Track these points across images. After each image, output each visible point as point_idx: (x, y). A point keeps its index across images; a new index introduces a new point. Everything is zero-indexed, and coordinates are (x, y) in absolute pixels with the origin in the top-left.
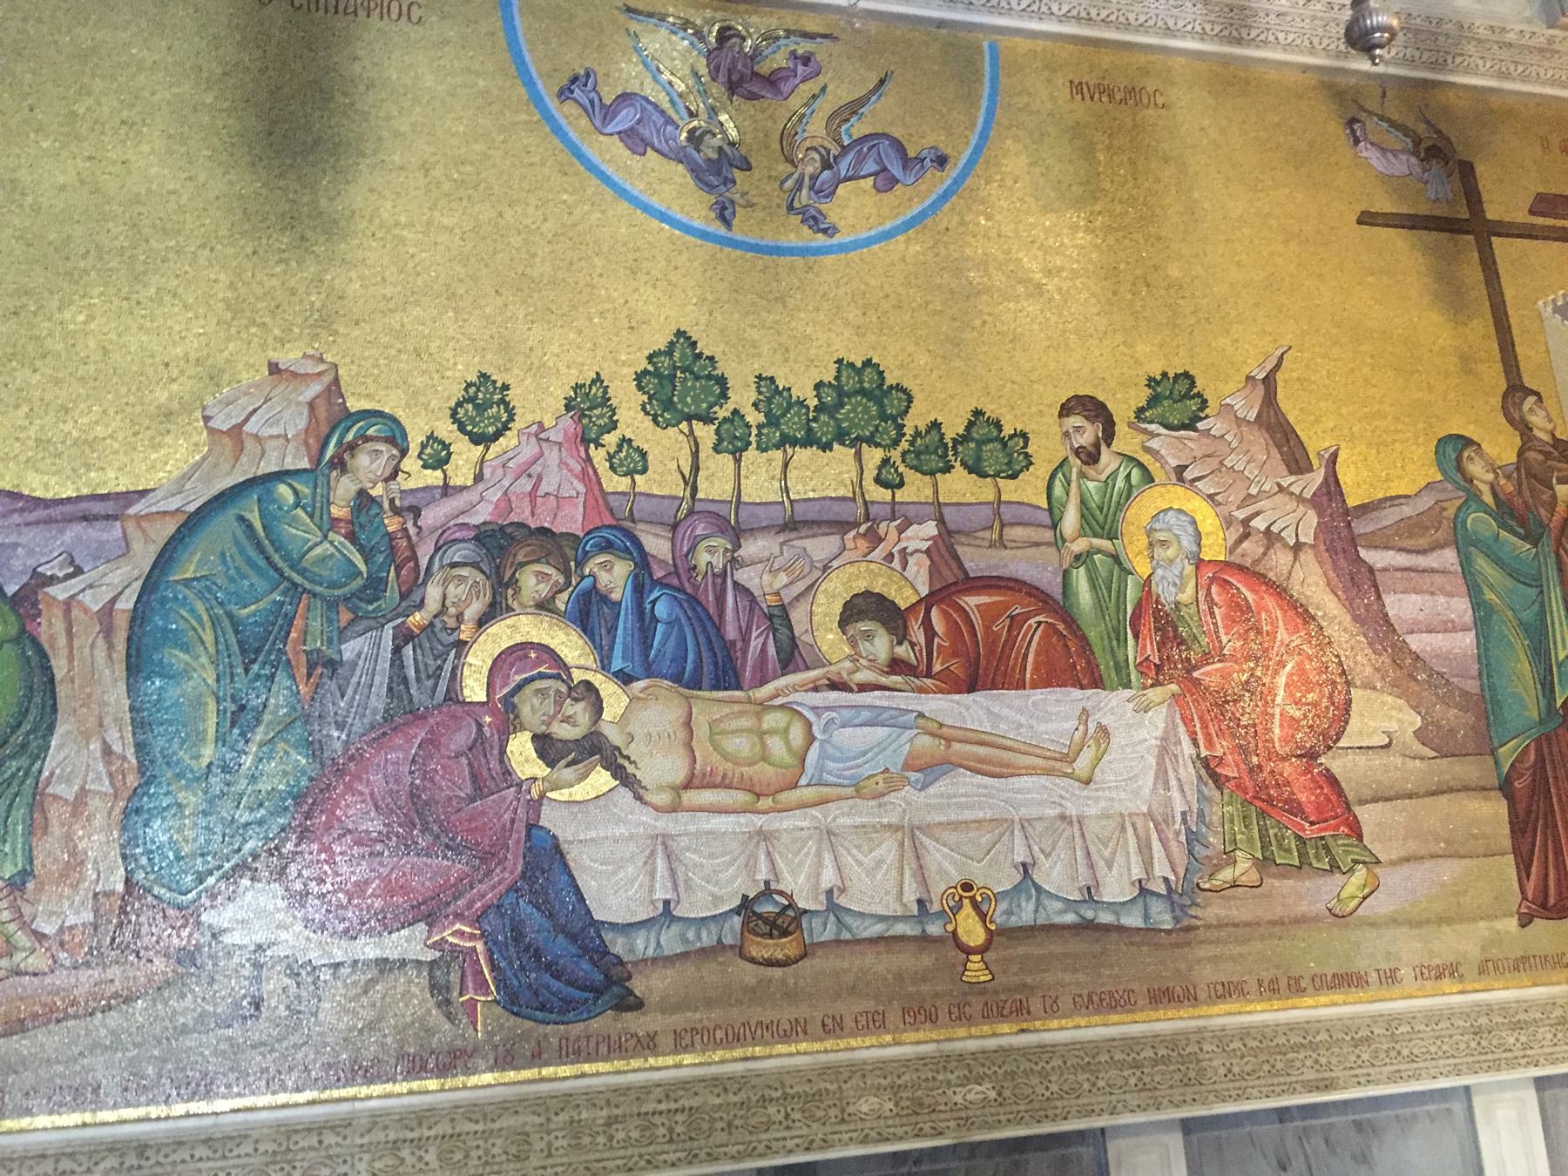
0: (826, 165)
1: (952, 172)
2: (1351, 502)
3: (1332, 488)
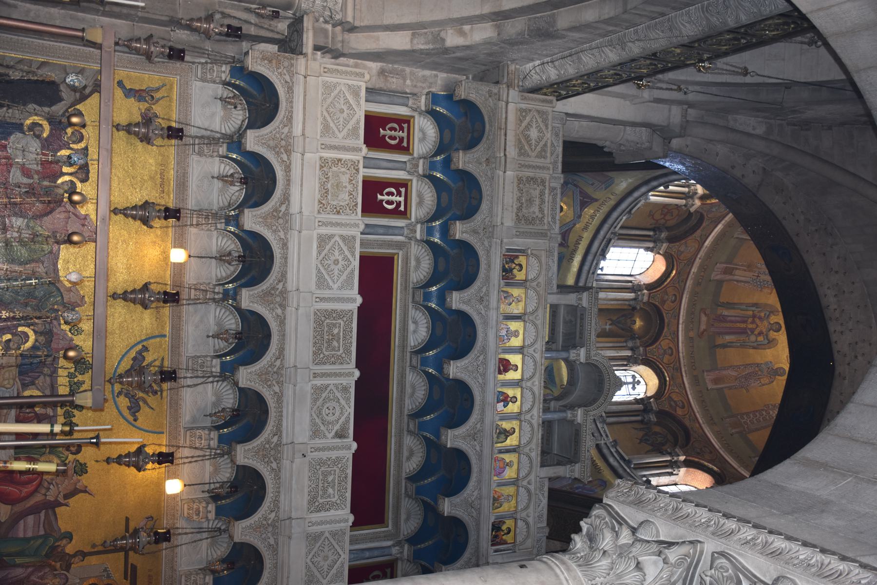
0: (133, 396)
1: (133, 422)
2: (57, 510)
3: (60, 505)
